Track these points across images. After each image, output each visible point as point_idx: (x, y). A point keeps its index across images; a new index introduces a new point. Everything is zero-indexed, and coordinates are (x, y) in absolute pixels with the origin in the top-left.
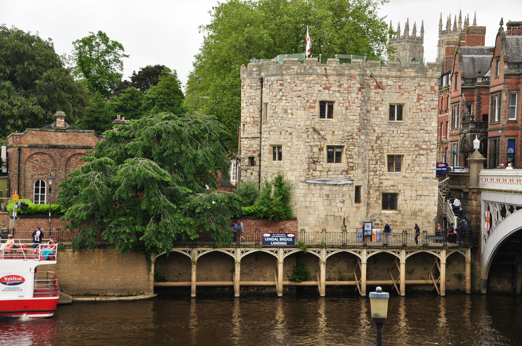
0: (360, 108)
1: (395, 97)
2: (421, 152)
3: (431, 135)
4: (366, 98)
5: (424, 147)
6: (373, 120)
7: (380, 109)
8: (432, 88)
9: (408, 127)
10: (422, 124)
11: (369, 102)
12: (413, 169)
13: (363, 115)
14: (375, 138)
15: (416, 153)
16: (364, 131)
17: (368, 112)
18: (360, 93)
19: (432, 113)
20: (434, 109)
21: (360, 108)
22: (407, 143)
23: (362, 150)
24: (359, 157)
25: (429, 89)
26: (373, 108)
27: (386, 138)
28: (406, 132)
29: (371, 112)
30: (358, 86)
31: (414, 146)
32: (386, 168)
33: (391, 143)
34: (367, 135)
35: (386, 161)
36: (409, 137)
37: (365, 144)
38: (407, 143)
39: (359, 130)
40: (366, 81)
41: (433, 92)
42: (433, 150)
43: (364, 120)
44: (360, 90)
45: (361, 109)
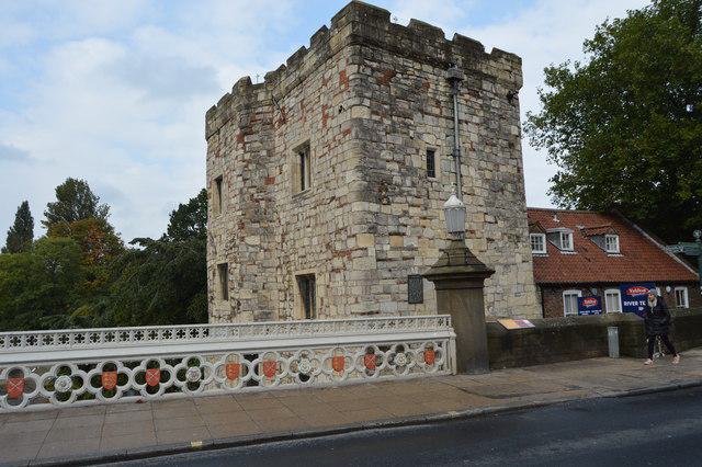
0: (240, 179)
1: (298, 131)
2: (337, 263)
3: (347, 208)
4: (264, 153)
5: (339, 247)
6: (278, 197)
7: (284, 169)
8: (344, 79)
9: (314, 199)
10: (333, 185)
11: (272, 159)
12: (327, 310)
13: (252, 191)
14: (278, 239)
15: (329, 268)
16: (257, 225)
17: (270, 180)
18: (241, 145)
19: (346, 147)
20: (348, 132)
21: (240, 179)
22: (315, 240)
23: (254, 269)
24: (241, 285)
25: (336, 80)
26: (278, 171)
27: (291, 236)
28: (313, 212)
29: (276, 182)
30: (238, 132)
31: (324, 249)
32: (297, 309)
33: (297, 246)
34: (268, 233)
35: (295, 290)
36: (316, 225)
37: (262, 255)
38: (315, 240)
39: (242, 226)
40: (257, 117)
41: (343, 87)
42: (354, 254)
43: (257, 201)
44: (240, 139)
45: (245, 180)
